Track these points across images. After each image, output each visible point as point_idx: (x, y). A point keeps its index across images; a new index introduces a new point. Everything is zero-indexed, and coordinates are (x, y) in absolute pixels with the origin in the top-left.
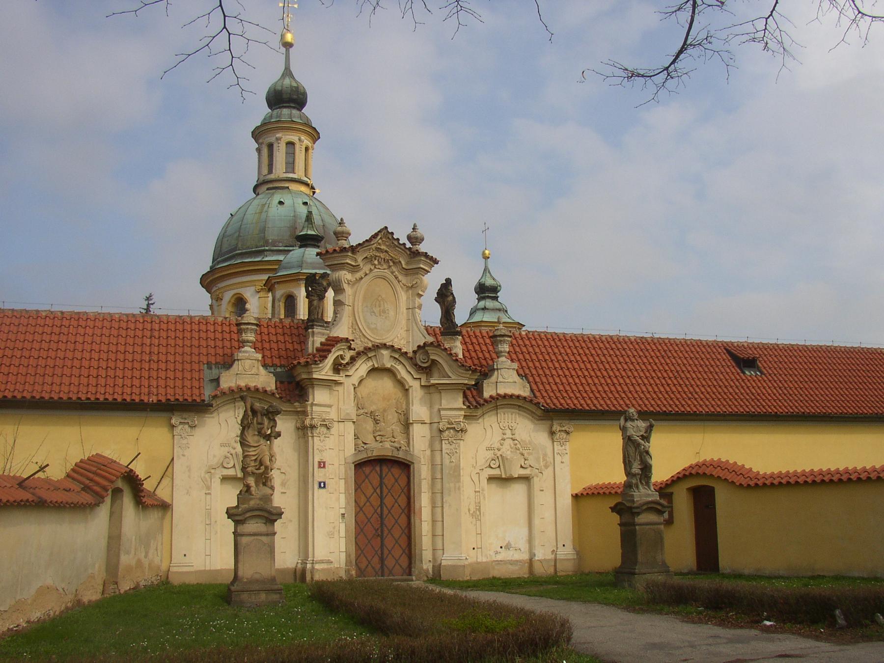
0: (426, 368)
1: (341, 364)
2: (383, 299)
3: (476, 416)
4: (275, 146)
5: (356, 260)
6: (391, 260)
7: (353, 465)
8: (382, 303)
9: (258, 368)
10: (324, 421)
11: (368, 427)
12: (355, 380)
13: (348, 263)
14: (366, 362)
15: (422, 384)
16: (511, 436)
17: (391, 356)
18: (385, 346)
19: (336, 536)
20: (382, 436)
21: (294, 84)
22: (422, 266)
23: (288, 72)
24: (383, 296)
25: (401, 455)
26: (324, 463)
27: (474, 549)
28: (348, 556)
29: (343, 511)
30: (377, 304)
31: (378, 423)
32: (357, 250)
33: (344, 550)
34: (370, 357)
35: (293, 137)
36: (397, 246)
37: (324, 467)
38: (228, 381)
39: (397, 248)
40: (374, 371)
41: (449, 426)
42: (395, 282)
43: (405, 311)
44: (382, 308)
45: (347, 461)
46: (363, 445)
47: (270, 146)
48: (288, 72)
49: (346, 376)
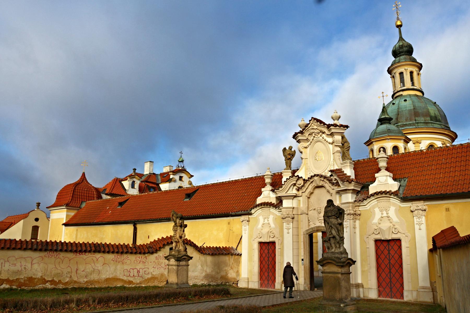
4: (395, 76)
6: (321, 132)
7: (307, 235)
13: (299, 139)
14: (311, 184)
16: (386, 215)
18: (315, 175)
22: (333, 131)
23: (401, 39)
31: (319, 214)
32: (304, 132)
34: (312, 182)
35: (401, 69)
38: (259, 200)
42: (325, 142)
43: (332, 155)
47: (393, 77)
48: (401, 39)
49: (302, 192)
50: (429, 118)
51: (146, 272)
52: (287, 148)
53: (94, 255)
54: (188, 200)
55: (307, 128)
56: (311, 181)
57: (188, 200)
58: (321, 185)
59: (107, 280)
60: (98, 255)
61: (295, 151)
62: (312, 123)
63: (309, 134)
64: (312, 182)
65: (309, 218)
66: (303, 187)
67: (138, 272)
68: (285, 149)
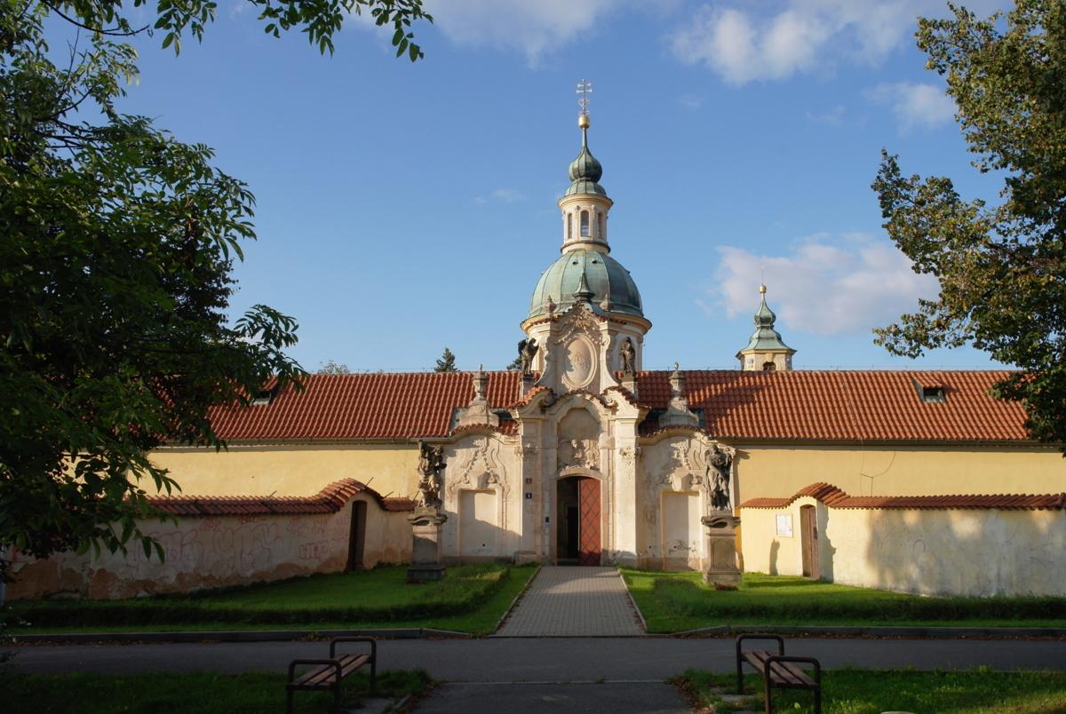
0: (610, 407)
1: (545, 407)
21: (589, 160)
25: (592, 474)
26: (531, 480)
28: (551, 548)
37: (531, 482)
50: (626, 299)
51: (325, 550)
53: (265, 522)
54: (266, 403)
56: (568, 398)
57: (266, 403)
58: (583, 406)
59: (280, 567)
60: (270, 521)
67: (316, 548)
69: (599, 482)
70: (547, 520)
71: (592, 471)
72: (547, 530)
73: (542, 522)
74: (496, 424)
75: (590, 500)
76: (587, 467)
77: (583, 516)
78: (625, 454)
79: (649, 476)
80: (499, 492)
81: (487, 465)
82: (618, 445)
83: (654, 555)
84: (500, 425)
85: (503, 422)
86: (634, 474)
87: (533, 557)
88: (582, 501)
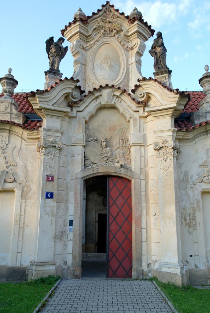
0: (142, 102)
1: (72, 102)
2: (109, 58)
3: (189, 139)
5: (88, 32)
6: (115, 29)
7: (82, 180)
8: (109, 60)
9: (11, 109)
10: (52, 142)
11: (96, 151)
12: (86, 114)
15: (140, 115)
17: (114, 95)
19: (65, 239)
20: (108, 157)
24: (110, 56)
27: (191, 256)
28: (74, 257)
29: (71, 218)
30: (106, 61)
33: (71, 252)
34: (97, 97)
36: (118, 17)
37: (52, 180)
39: (118, 19)
40: (102, 108)
41: (163, 145)
44: (109, 64)
45: (77, 177)
46: (92, 165)
49: (77, 111)
52: (56, 40)
55: (95, 16)
56: (97, 94)
58: (113, 103)
61: (67, 47)
62: (105, 12)
63: (95, 29)
64: (97, 97)
65: (86, 153)
66: (81, 103)
68: (52, 39)
69: (130, 181)
70: (71, 223)
71: (122, 169)
72: (71, 235)
73: (65, 225)
74: (20, 121)
75: (120, 201)
76: (118, 165)
77: (111, 219)
78: (160, 148)
79: (186, 175)
80: (18, 192)
81: (7, 163)
82: (151, 139)
83: (196, 266)
84: (24, 123)
85: (29, 122)
86: (172, 170)
87: (51, 270)
88: (111, 202)
